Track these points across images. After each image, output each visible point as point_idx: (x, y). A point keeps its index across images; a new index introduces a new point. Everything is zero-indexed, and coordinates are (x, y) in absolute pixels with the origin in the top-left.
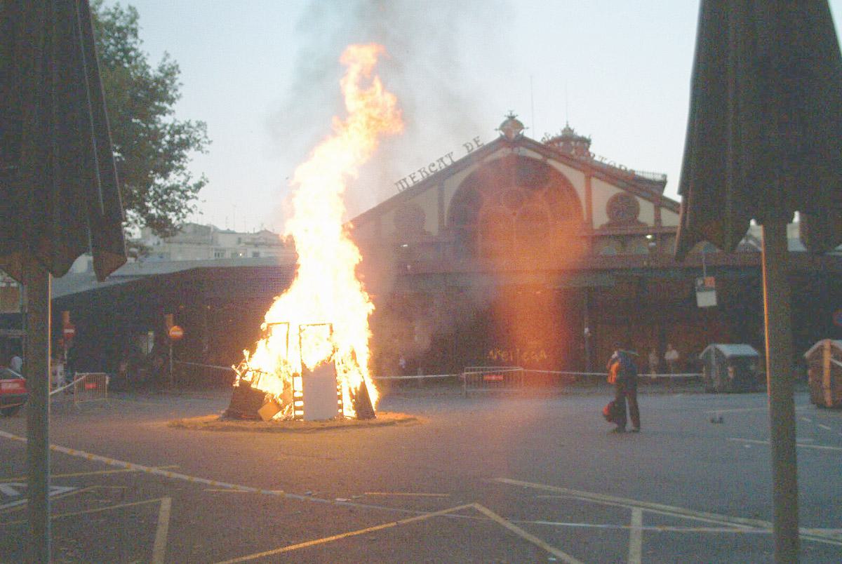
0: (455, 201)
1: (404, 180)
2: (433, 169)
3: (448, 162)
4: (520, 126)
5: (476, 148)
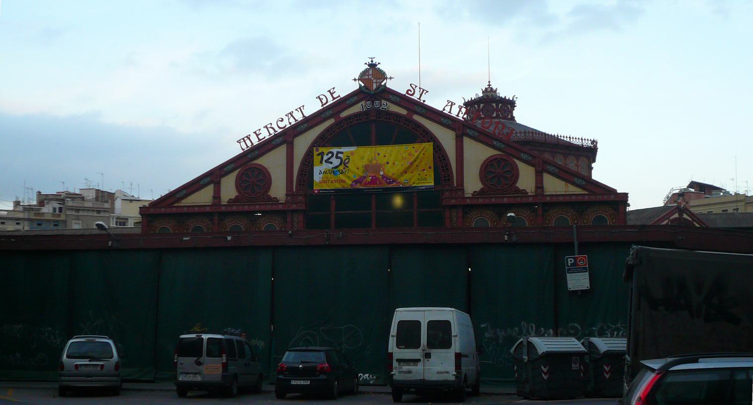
1: (248, 137)
2: (282, 125)
3: (299, 117)
4: (382, 75)
5: (331, 101)
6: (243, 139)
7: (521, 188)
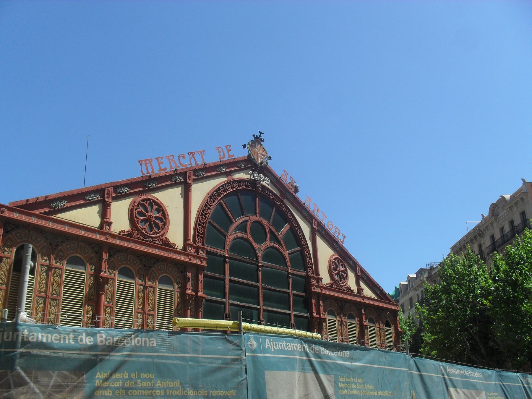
1: (150, 161)
5: (226, 158)
6: (145, 161)
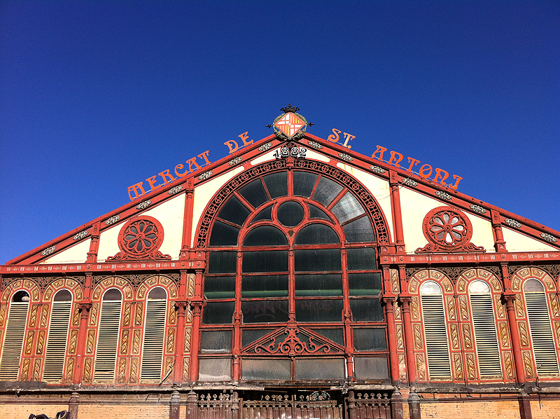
0: (207, 215)
7: (477, 245)
